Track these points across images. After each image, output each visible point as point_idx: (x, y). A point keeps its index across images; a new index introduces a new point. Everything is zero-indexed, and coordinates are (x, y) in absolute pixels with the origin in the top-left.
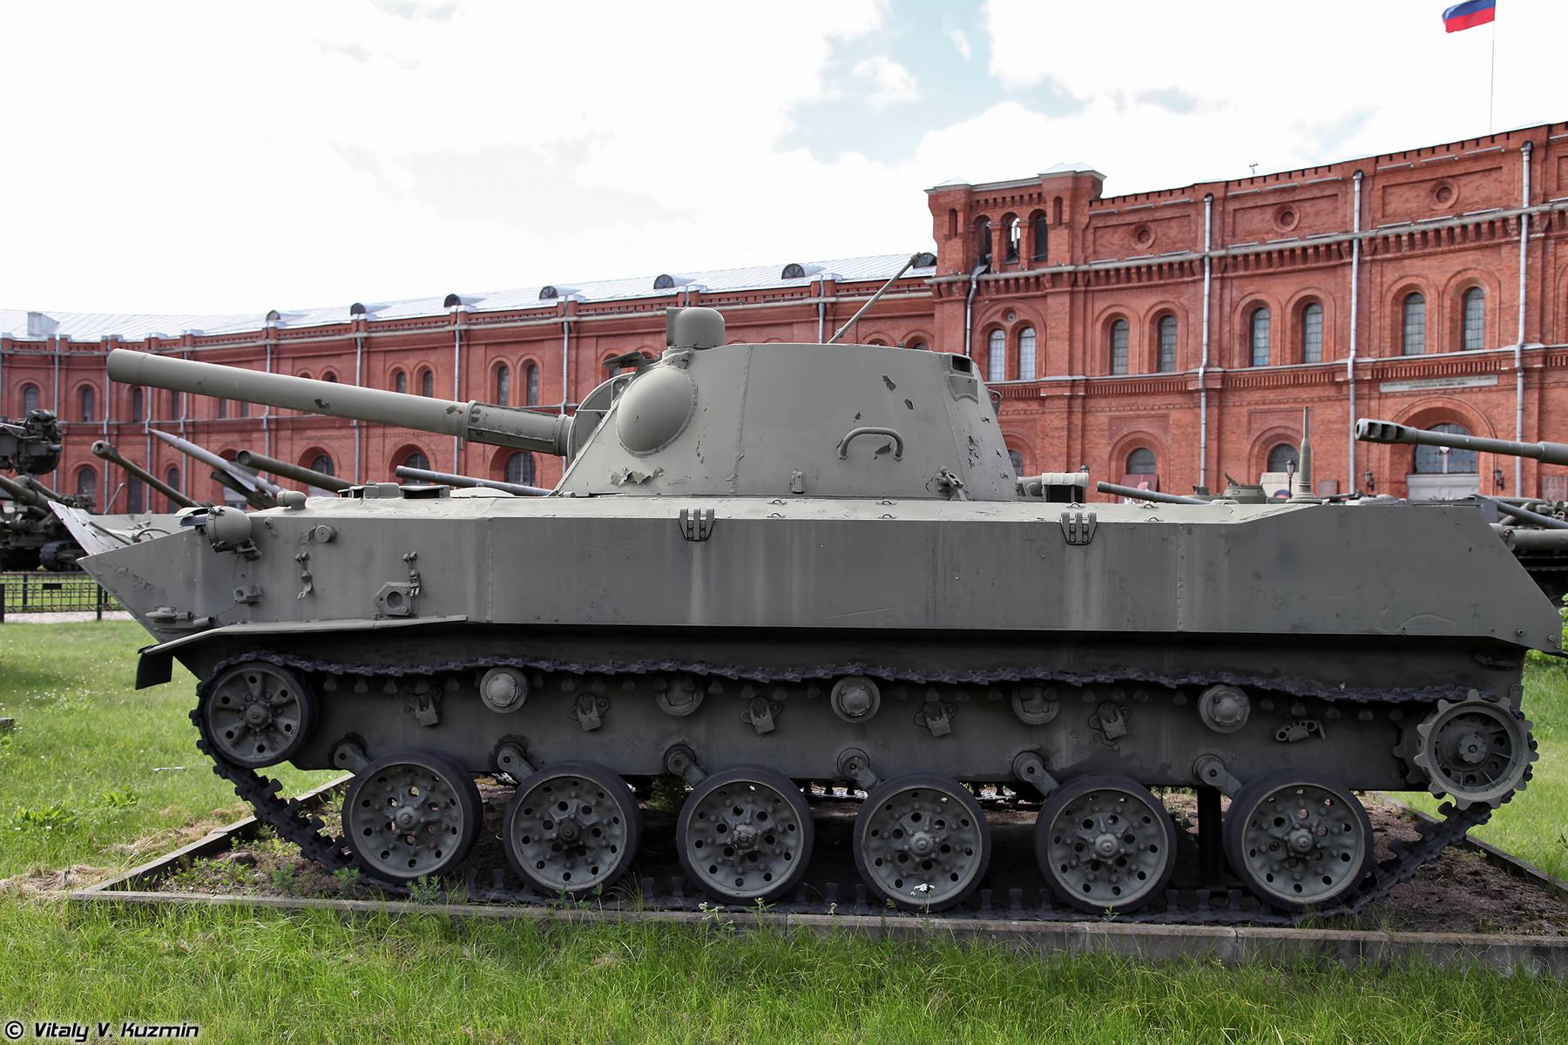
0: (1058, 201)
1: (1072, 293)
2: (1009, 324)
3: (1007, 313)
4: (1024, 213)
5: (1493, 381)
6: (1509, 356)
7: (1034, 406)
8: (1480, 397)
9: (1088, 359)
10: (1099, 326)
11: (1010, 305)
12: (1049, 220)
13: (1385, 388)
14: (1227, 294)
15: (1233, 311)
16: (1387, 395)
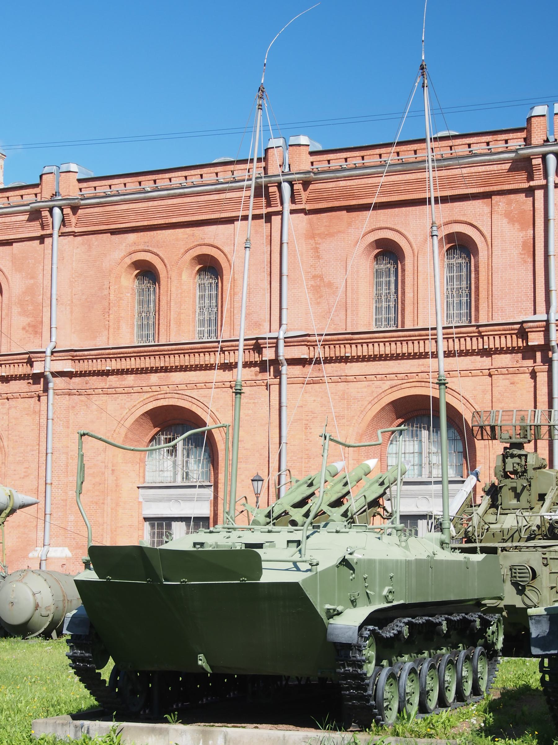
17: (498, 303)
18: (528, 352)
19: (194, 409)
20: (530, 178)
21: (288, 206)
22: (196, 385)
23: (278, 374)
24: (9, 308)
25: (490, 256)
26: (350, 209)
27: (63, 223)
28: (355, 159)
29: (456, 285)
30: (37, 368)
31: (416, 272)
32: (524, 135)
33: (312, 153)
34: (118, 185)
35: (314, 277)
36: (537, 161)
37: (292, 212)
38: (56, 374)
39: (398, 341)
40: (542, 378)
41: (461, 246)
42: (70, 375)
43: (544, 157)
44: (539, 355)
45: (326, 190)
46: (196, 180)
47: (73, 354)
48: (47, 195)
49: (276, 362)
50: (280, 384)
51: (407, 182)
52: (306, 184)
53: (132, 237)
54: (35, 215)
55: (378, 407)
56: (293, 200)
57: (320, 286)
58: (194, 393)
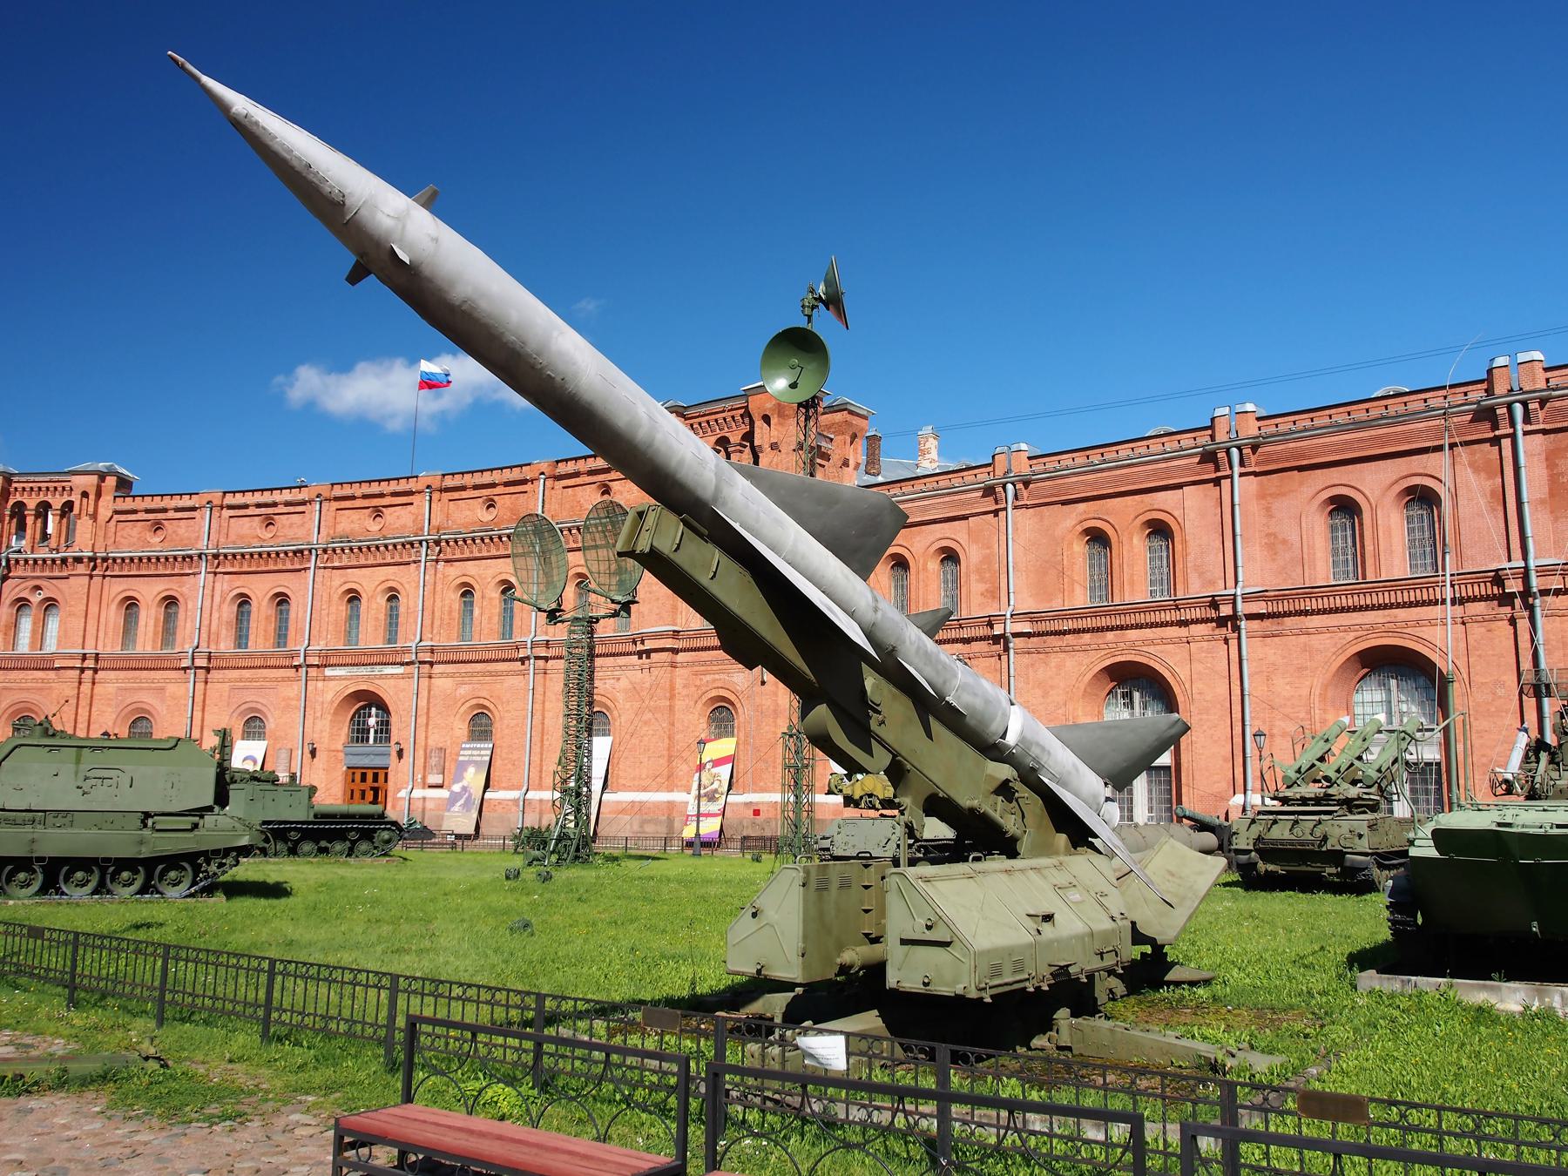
0: (85, 495)
1: (91, 577)
2: (36, 598)
3: (38, 588)
4: (57, 502)
5: (400, 670)
6: (406, 650)
7: (52, 674)
8: (392, 682)
9: (101, 635)
10: (114, 606)
11: (38, 582)
12: (76, 510)
13: (328, 672)
14: (218, 585)
15: (223, 600)
16: (331, 679)
17: (1467, 552)
18: (1506, 599)
19: (1152, 663)
20: (1495, 427)
21: (1237, 470)
22: (1152, 642)
23: (1237, 629)
24: (968, 576)
25: (1455, 506)
26: (1300, 469)
27: (1016, 497)
28: (1304, 422)
29: (1417, 535)
30: (998, 630)
31: (1375, 526)
32: (1485, 386)
33: (1258, 419)
34: (1066, 460)
35: (1268, 535)
36: (1502, 411)
37: (1241, 475)
38: (1016, 635)
39: (1360, 592)
40: (1523, 624)
41: (1422, 498)
42: (1028, 635)
43: (1509, 406)
44: (1518, 602)
45: (1276, 452)
46: (1143, 451)
47: (1030, 616)
48: (999, 473)
49: (1234, 618)
50: (1239, 638)
51: (1362, 440)
52: (1255, 448)
53: (1082, 506)
54: (989, 491)
55: (1342, 658)
56: (1242, 464)
57: (1274, 543)
58: (1151, 649)
